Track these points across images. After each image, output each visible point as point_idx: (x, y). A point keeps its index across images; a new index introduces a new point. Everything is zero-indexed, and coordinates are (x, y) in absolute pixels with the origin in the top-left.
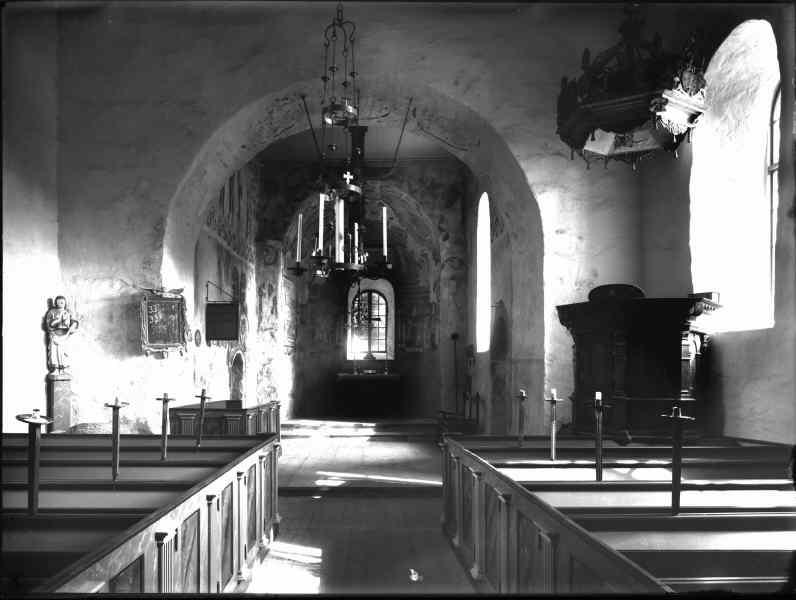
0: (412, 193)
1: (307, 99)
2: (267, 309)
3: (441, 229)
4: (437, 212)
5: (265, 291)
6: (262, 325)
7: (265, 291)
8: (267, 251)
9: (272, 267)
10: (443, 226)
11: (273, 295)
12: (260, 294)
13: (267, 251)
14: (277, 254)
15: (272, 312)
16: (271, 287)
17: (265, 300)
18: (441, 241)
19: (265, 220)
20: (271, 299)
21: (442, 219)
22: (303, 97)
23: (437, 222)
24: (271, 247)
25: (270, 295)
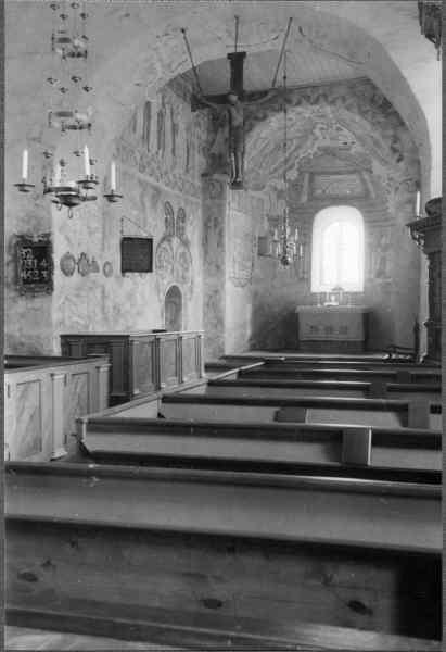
1: (187, 32)
3: (394, 150)
5: (211, 224)
9: (217, 201)
12: (206, 226)
14: (222, 187)
16: (216, 219)
19: (213, 154)
20: (217, 231)
22: (183, 31)
24: (217, 181)
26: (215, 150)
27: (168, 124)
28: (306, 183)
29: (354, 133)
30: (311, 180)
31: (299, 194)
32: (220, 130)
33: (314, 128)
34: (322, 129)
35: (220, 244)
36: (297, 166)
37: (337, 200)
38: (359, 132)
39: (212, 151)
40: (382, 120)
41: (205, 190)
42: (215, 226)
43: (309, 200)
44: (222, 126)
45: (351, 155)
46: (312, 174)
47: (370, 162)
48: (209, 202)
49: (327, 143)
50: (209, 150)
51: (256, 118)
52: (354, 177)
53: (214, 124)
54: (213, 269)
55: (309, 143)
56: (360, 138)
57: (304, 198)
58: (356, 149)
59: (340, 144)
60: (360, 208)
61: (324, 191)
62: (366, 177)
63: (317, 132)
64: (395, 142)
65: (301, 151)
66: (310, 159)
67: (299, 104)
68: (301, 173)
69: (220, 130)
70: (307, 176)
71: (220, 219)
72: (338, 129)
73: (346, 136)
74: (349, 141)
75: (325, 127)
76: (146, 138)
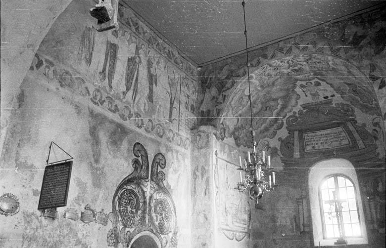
0: (335, 53)
2: (201, 190)
4: (366, 62)
5: (199, 174)
6: (196, 207)
7: (199, 174)
8: (200, 136)
9: (203, 151)
10: (377, 73)
11: (205, 177)
13: (200, 136)
14: (208, 135)
15: (205, 194)
16: (203, 168)
17: (199, 181)
18: (376, 89)
19: (202, 112)
21: (373, 67)
23: (367, 71)
24: (204, 132)
25: (202, 175)
26: (204, 108)
27: (143, 73)
28: (296, 142)
29: (331, 85)
30: (301, 138)
31: (292, 151)
32: (207, 90)
33: (295, 86)
34: (302, 86)
35: (207, 192)
36: (285, 125)
37: (327, 155)
38: (337, 82)
39: (201, 109)
40: (356, 53)
41: (194, 141)
42: (202, 175)
43: (302, 156)
44: (209, 87)
45: (333, 108)
46: (301, 132)
47: (353, 111)
48: (196, 153)
49: (310, 100)
50: (199, 108)
51: (238, 76)
52: (340, 129)
53: (202, 86)
54: (201, 219)
55: (293, 102)
56: (338, 90)
57: (297, 155)
58: (338, 99)
59: (322, 99)
60: (350, 159)
61: (314, 147)
62: (351, 128)
63: (298, 90)
64: (374, 70)
65: (286, 111)
66: (297, 117)
67: (273, 56)
68: (291, 132)
69: (207, 90)
70: (296, 134)
71: (206, 168)
72: (318, 84)
73: (325, 90)
74: (329, 94)
75: (304, 83)
76: (108, 73)
